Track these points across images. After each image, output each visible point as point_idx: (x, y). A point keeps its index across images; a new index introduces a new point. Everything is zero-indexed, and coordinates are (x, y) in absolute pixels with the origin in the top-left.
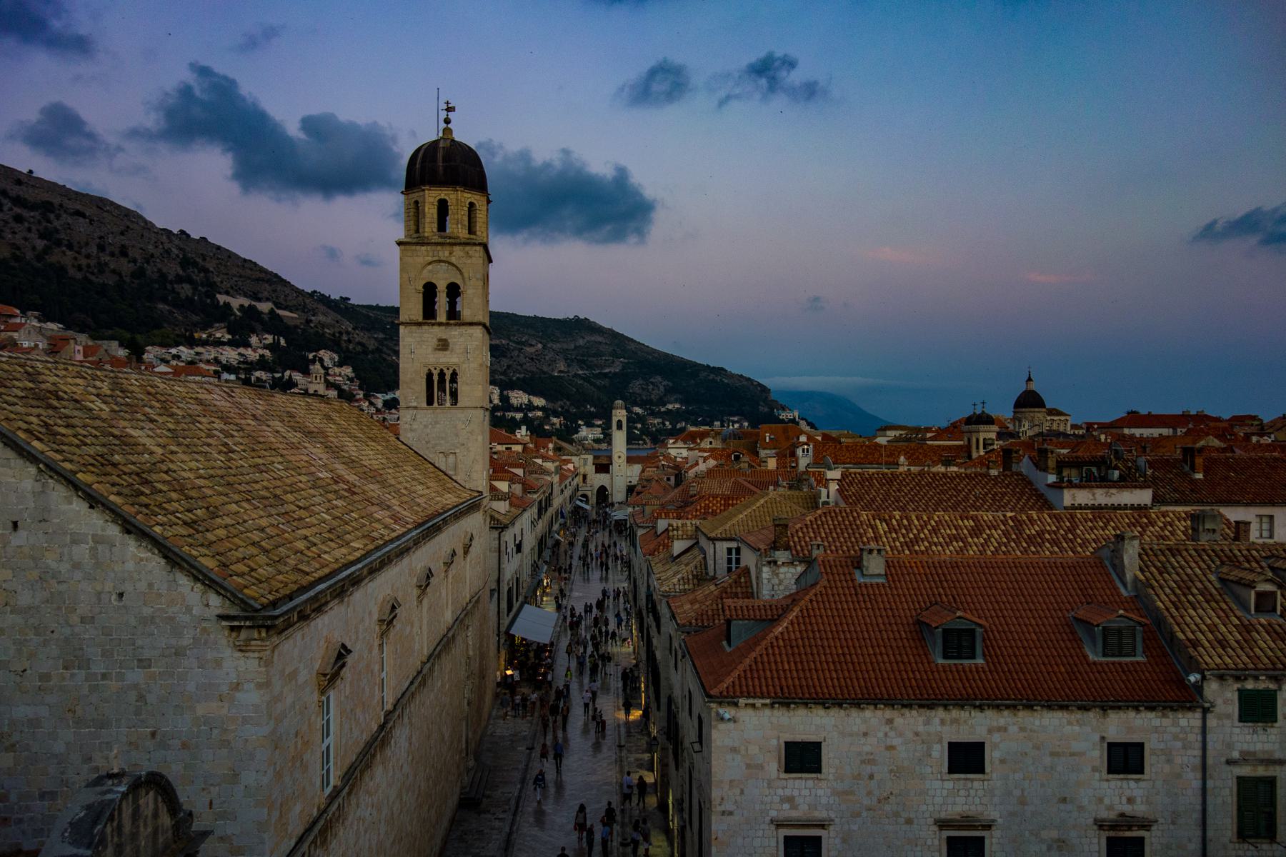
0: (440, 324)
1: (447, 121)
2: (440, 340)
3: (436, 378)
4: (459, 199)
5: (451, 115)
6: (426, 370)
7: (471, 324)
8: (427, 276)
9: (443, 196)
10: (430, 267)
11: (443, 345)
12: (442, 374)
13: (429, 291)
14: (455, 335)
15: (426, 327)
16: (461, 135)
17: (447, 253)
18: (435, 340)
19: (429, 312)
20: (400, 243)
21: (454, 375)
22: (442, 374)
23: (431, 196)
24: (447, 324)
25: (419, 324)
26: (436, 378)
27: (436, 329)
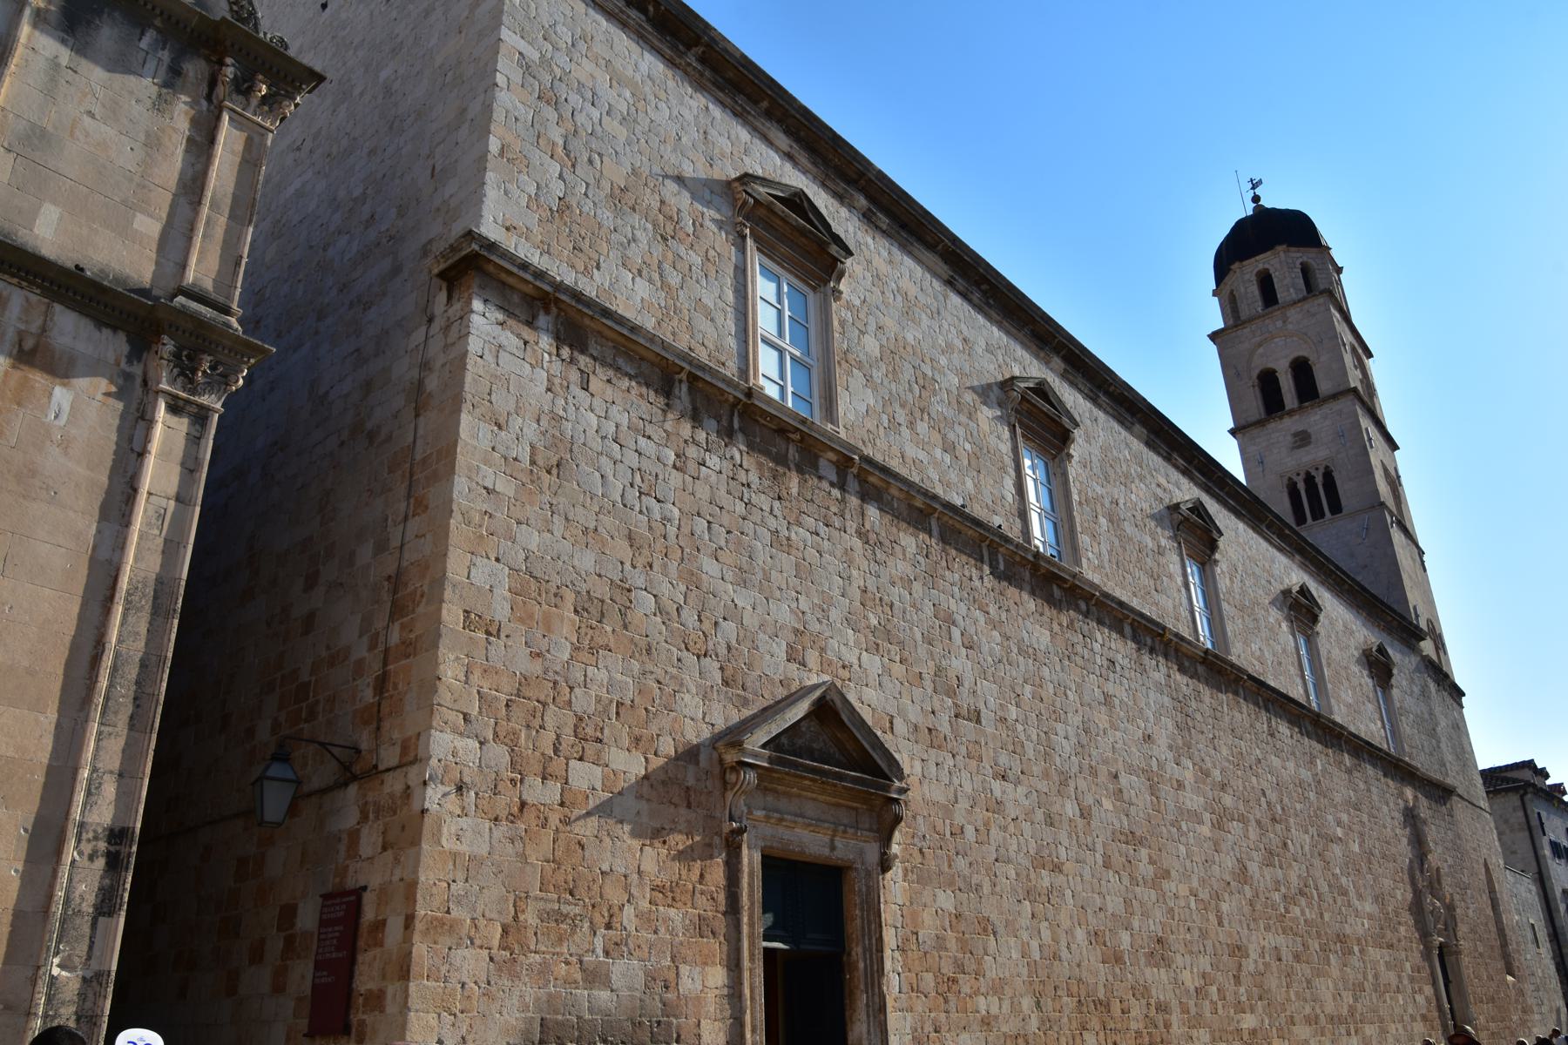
0: (1291, 413)
1: (1256, 199)
2: (1296, 435)
3: (1301, 486)
4: (1281, 263)
5: (1258, 191)
6: (1285, 481)
7: (1335, 396)
8: (1259, 364)
9: (1261, 266)
10: (1261, 350)
11: (1302, 439)
12: (1309, 479)
13: (1268, 381)
14: (1317, 420)
15: (1272, 425)
16: (1273, 199)
17: (1279, 324)
18: (1289, 438)
19: (1273, 403)
20: (1214, 337)
21: (1328, 476)
22: (1309, 479)
23: (1245, 274)
24: (1300, 408)
25: (1260, 423)
26: (1301, 486)
27: (1287, 421)
